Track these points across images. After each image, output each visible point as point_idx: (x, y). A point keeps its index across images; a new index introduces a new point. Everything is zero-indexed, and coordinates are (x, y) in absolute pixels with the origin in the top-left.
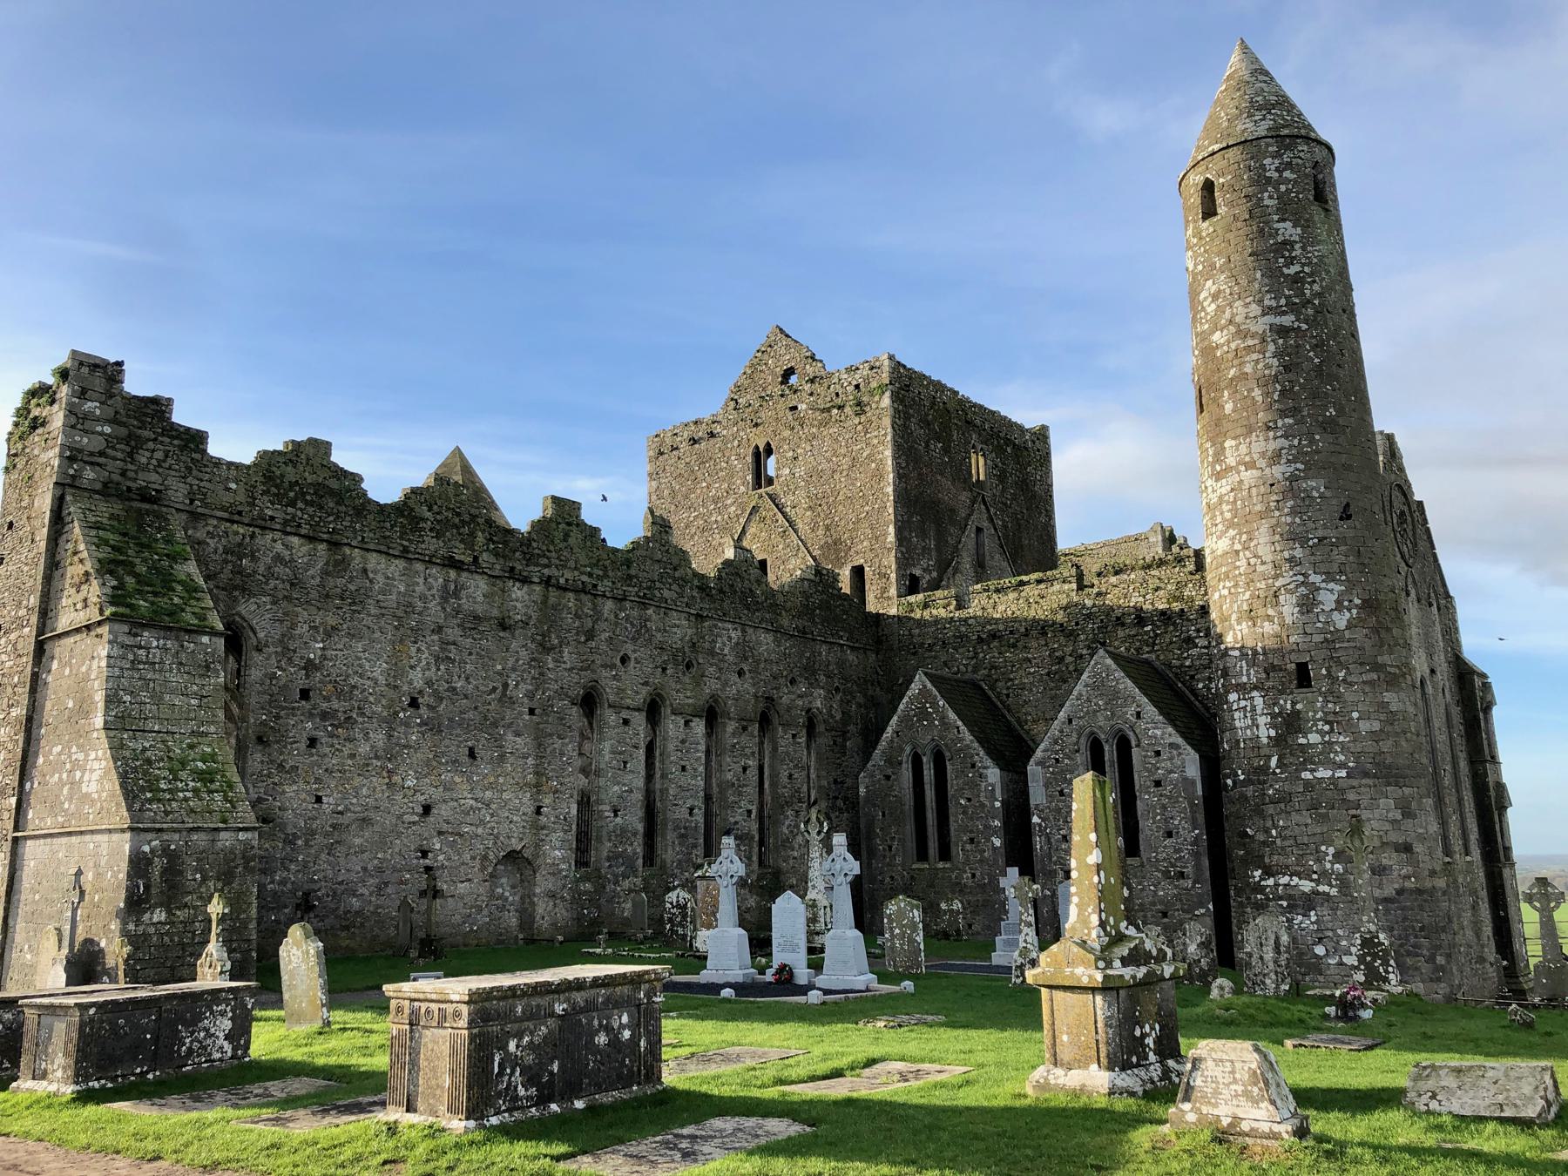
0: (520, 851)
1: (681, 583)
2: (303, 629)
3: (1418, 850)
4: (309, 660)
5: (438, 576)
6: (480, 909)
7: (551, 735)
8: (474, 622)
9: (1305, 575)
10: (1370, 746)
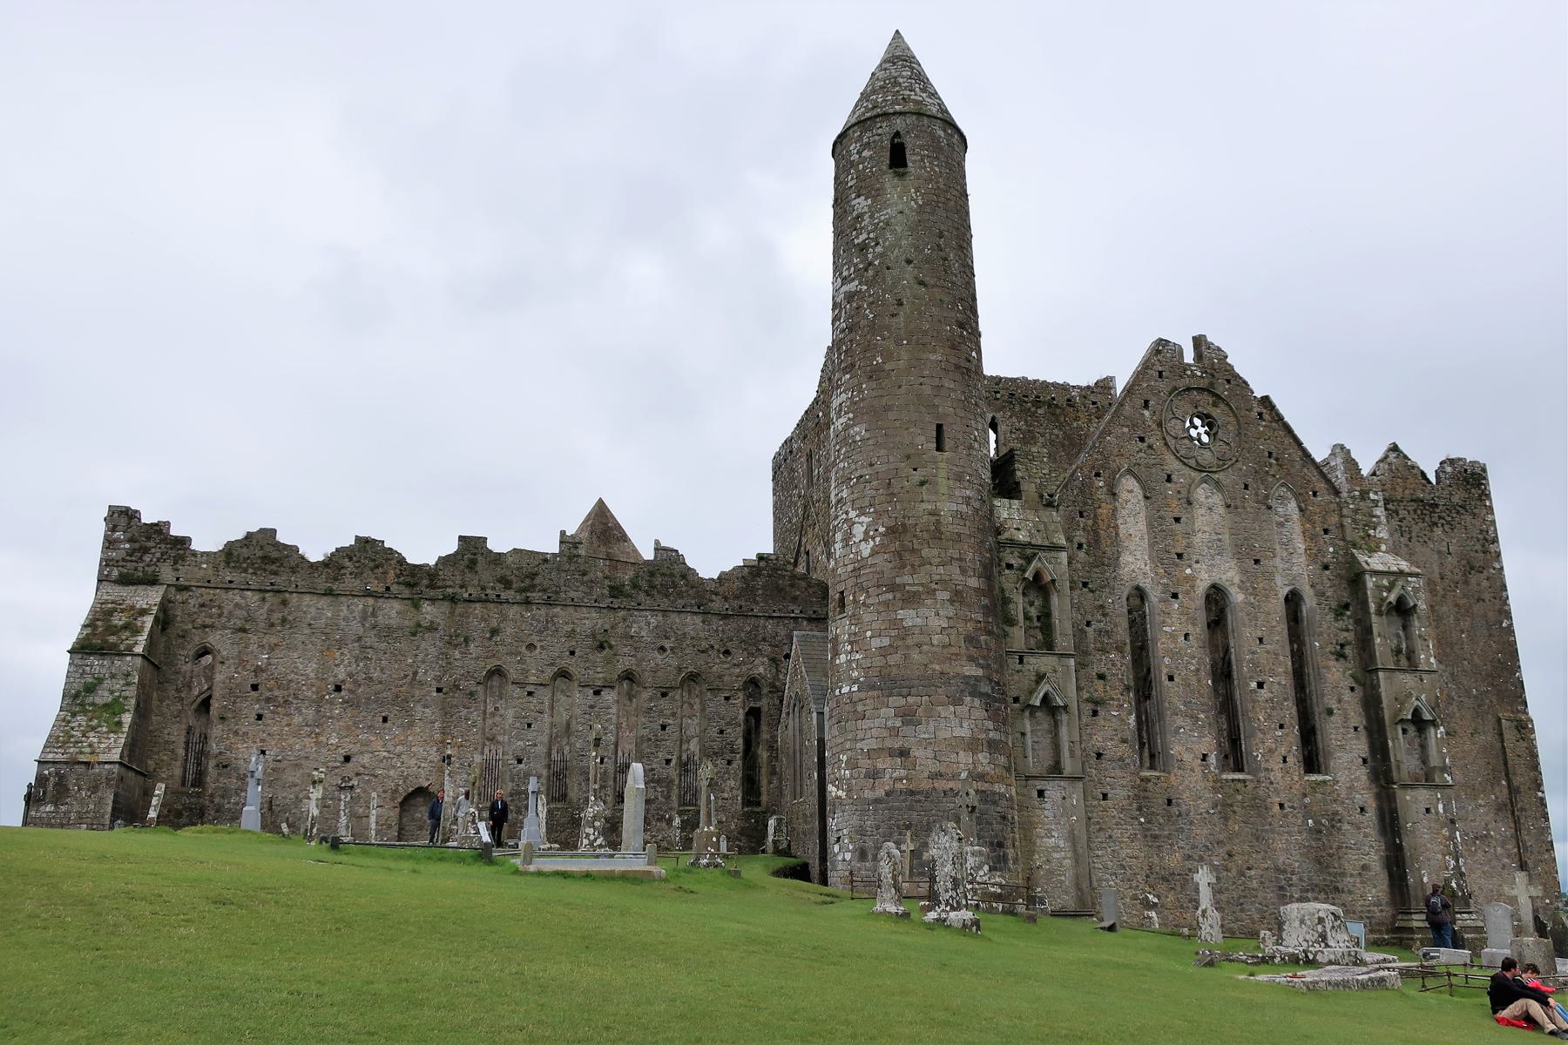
0: (427, 788)
1: (590, 584)
2: (253, 647)
3: (917, 754)
4: (258, 666)
5: (359, 605)
6: (390, 827)
7: (457, 706)
8: (387, 633)
9: (847, 513)
10: (878, 661)
